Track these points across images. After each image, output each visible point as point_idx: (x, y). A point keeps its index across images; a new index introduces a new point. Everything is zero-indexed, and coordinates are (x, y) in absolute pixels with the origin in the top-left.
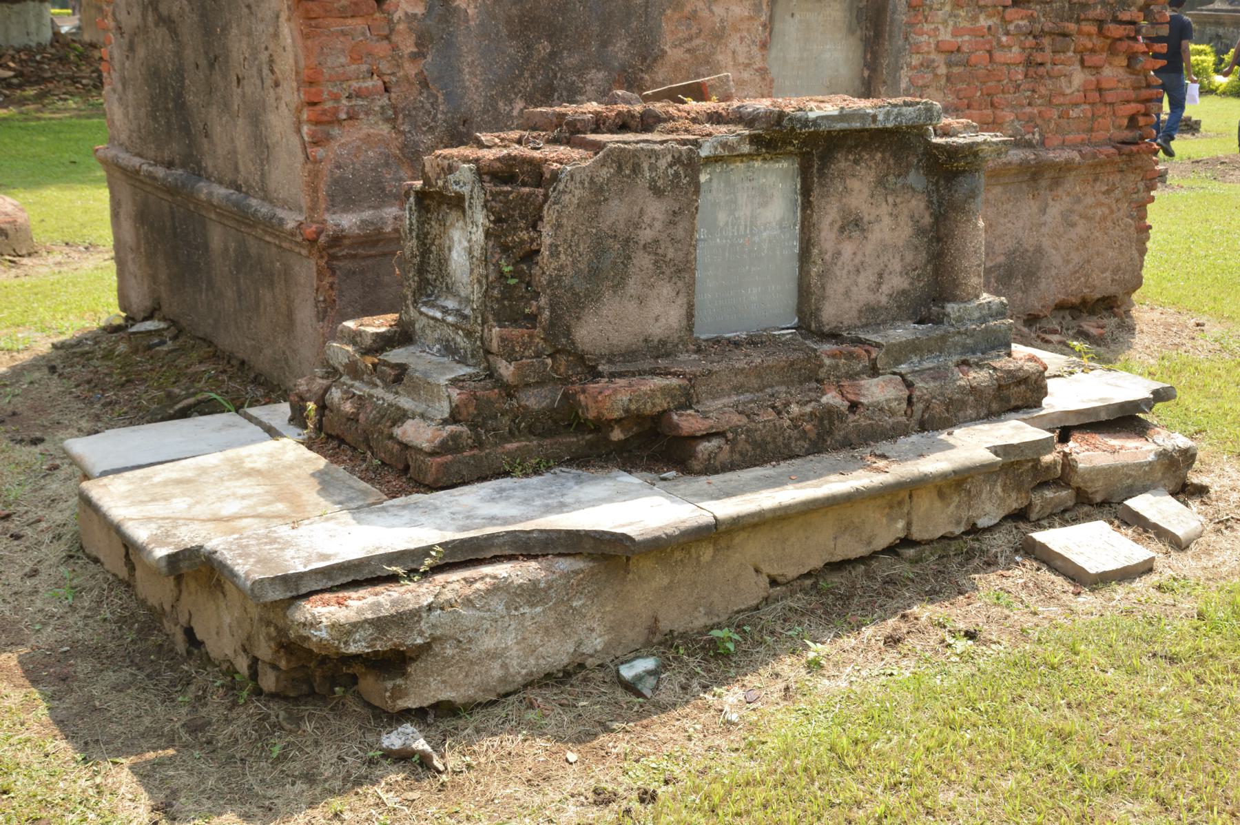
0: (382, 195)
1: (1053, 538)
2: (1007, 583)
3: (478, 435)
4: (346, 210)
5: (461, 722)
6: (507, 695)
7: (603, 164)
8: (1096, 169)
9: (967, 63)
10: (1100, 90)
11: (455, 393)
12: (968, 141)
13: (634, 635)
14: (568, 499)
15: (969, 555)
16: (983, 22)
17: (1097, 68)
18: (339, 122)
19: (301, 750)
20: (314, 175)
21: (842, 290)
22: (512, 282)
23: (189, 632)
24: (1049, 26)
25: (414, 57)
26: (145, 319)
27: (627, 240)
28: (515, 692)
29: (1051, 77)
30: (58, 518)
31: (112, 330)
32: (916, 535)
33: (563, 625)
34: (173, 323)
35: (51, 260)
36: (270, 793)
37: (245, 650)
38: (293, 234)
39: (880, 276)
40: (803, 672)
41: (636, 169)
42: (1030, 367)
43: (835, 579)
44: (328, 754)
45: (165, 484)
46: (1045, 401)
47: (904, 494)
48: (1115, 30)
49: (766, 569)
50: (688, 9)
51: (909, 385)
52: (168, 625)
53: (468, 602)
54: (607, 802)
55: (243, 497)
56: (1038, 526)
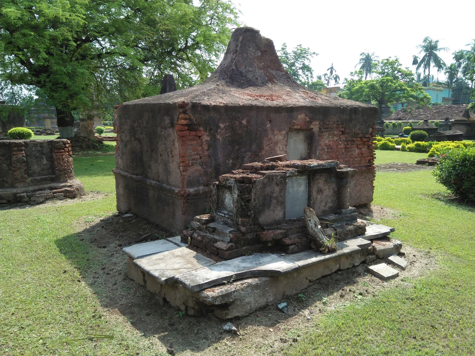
0: (199, 184)
1: (373, 268)
2: (365, 280)
3: (236, 245)
4: (191, 188)
5: (241, 322)
6: (251, 314)
7: (265, 178)
9: (332, 148)
10: (362, 154)
11: (231, 235)
12: (346, 170)
13: (279, 297)
14: (261, 262)
15: (354, 273)
16: (335, 138)
17: (361, 149)
18: (190, 166)
19: (202, 331)
20: (183, 179)
21: (318, 207)
22: (244, 207)
23: (165, 299)
24: (350, 139)
25: (207, 150)
26: (126, 213)
27: (271, 197)
28: (253, 313)
29: (351, 151)
30: (119, 269)
31: (115, 216)
32: (342, 268)
33: (264, 295)
34: (135, 214)
35: (89, 197)
36: (197, 343)
37: (184, 304)
38: (177, 193)
39: (326, 203)
40: (323, 305)
41: (273, 179)
42: (362, 224)
43: (324, 280)
44: (209, 332)
45: (156, 260)
46: (366, 233)
47: (339, 258)
48: (365, 140)
49: (309, 278)
50: (269, 137)
51: (336, 230)
52: (157, 297)
53: (242, 290)
54: (285, 342)
55: (179, 263)
56: (370, 265)
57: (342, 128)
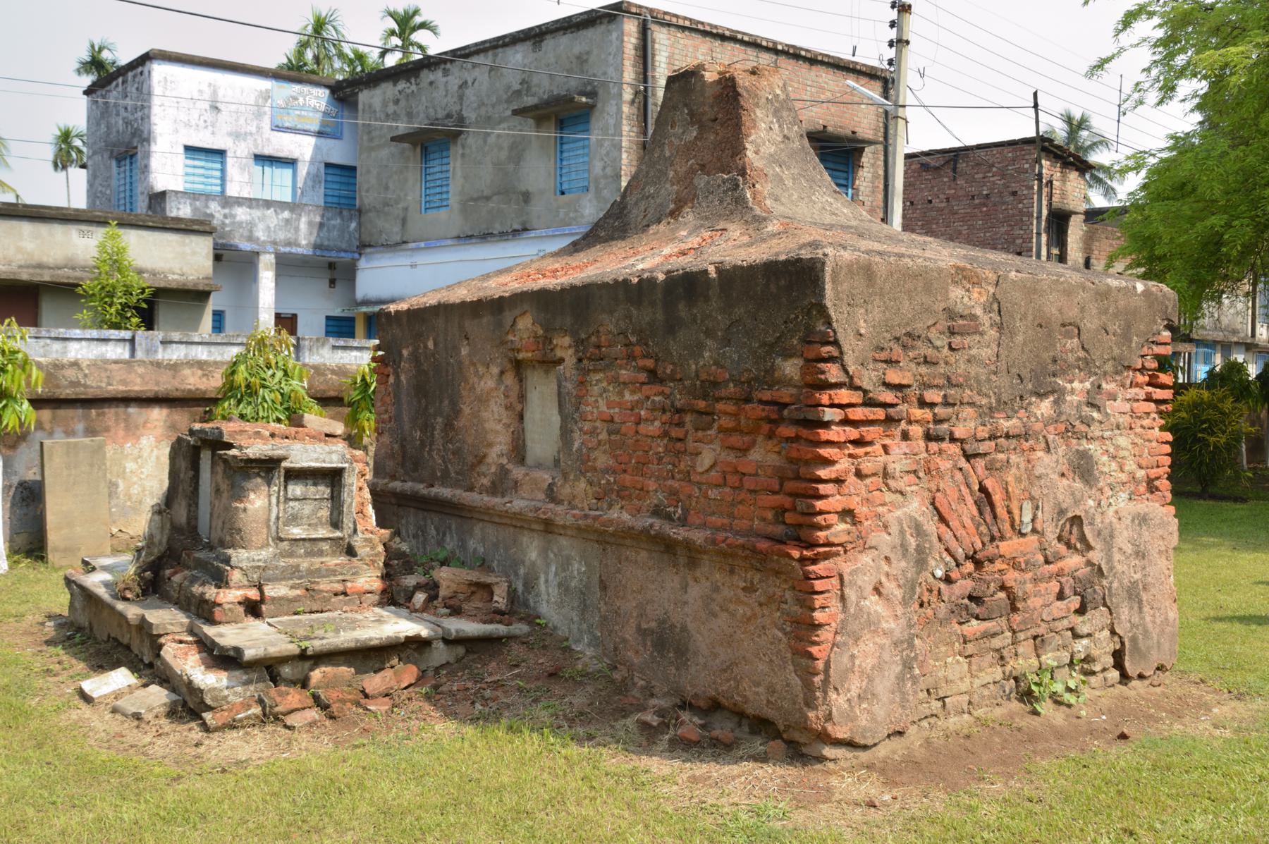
8: (729, 557)
57: (646, 356)
